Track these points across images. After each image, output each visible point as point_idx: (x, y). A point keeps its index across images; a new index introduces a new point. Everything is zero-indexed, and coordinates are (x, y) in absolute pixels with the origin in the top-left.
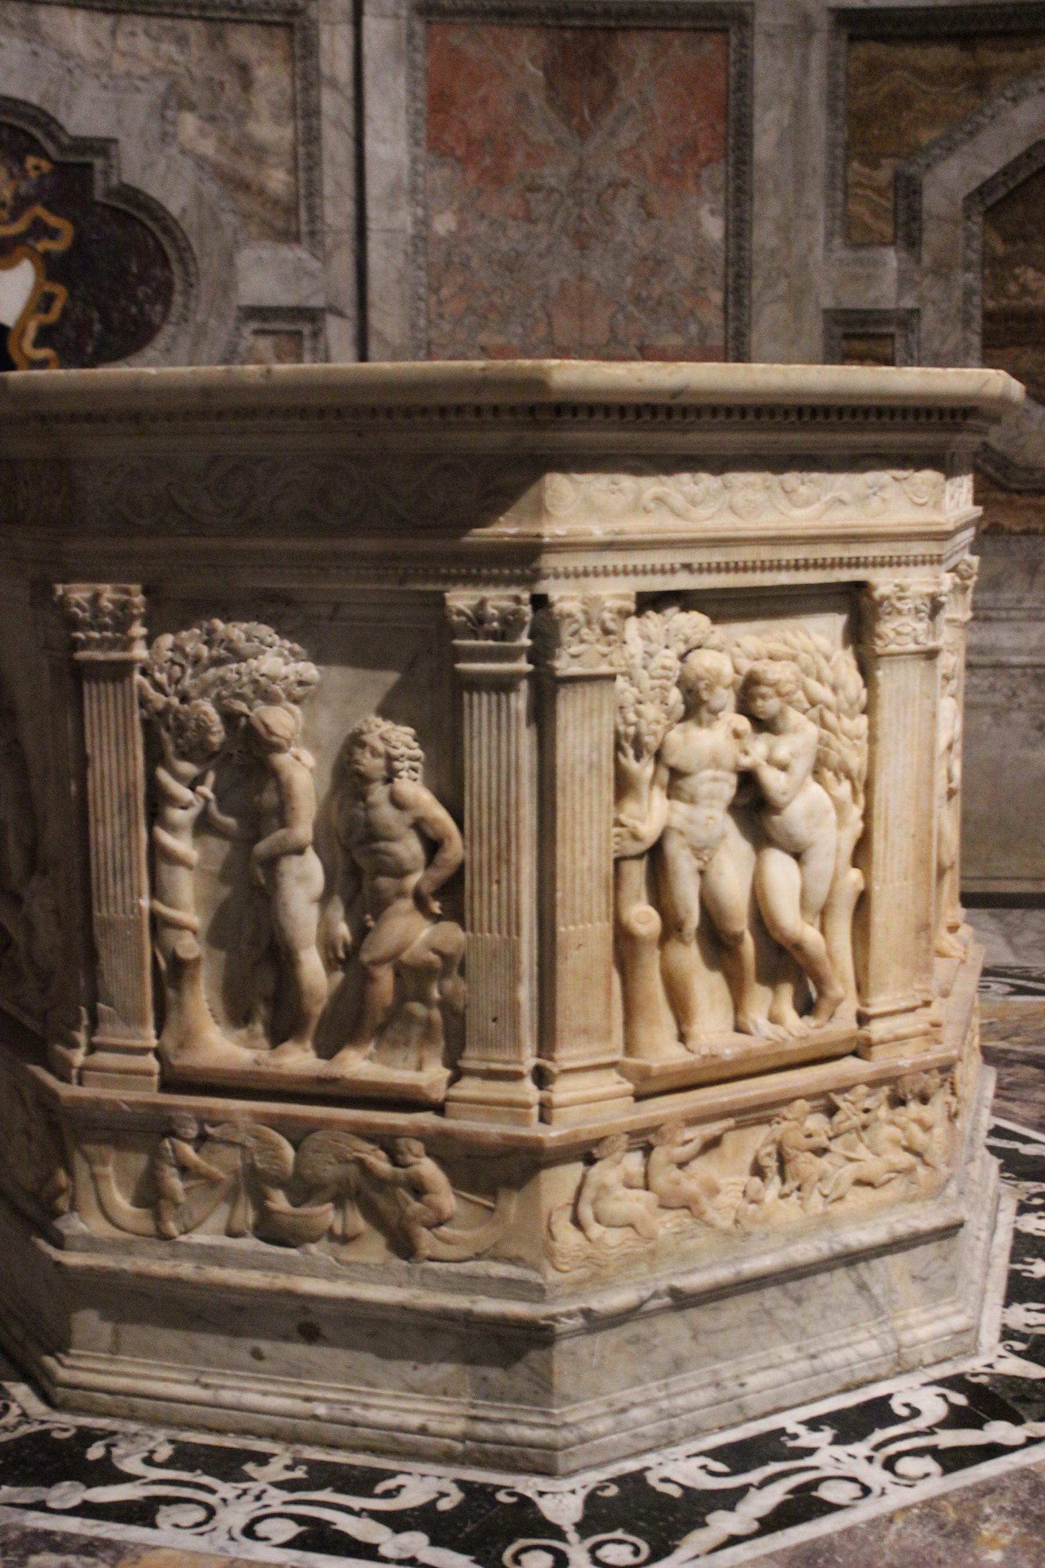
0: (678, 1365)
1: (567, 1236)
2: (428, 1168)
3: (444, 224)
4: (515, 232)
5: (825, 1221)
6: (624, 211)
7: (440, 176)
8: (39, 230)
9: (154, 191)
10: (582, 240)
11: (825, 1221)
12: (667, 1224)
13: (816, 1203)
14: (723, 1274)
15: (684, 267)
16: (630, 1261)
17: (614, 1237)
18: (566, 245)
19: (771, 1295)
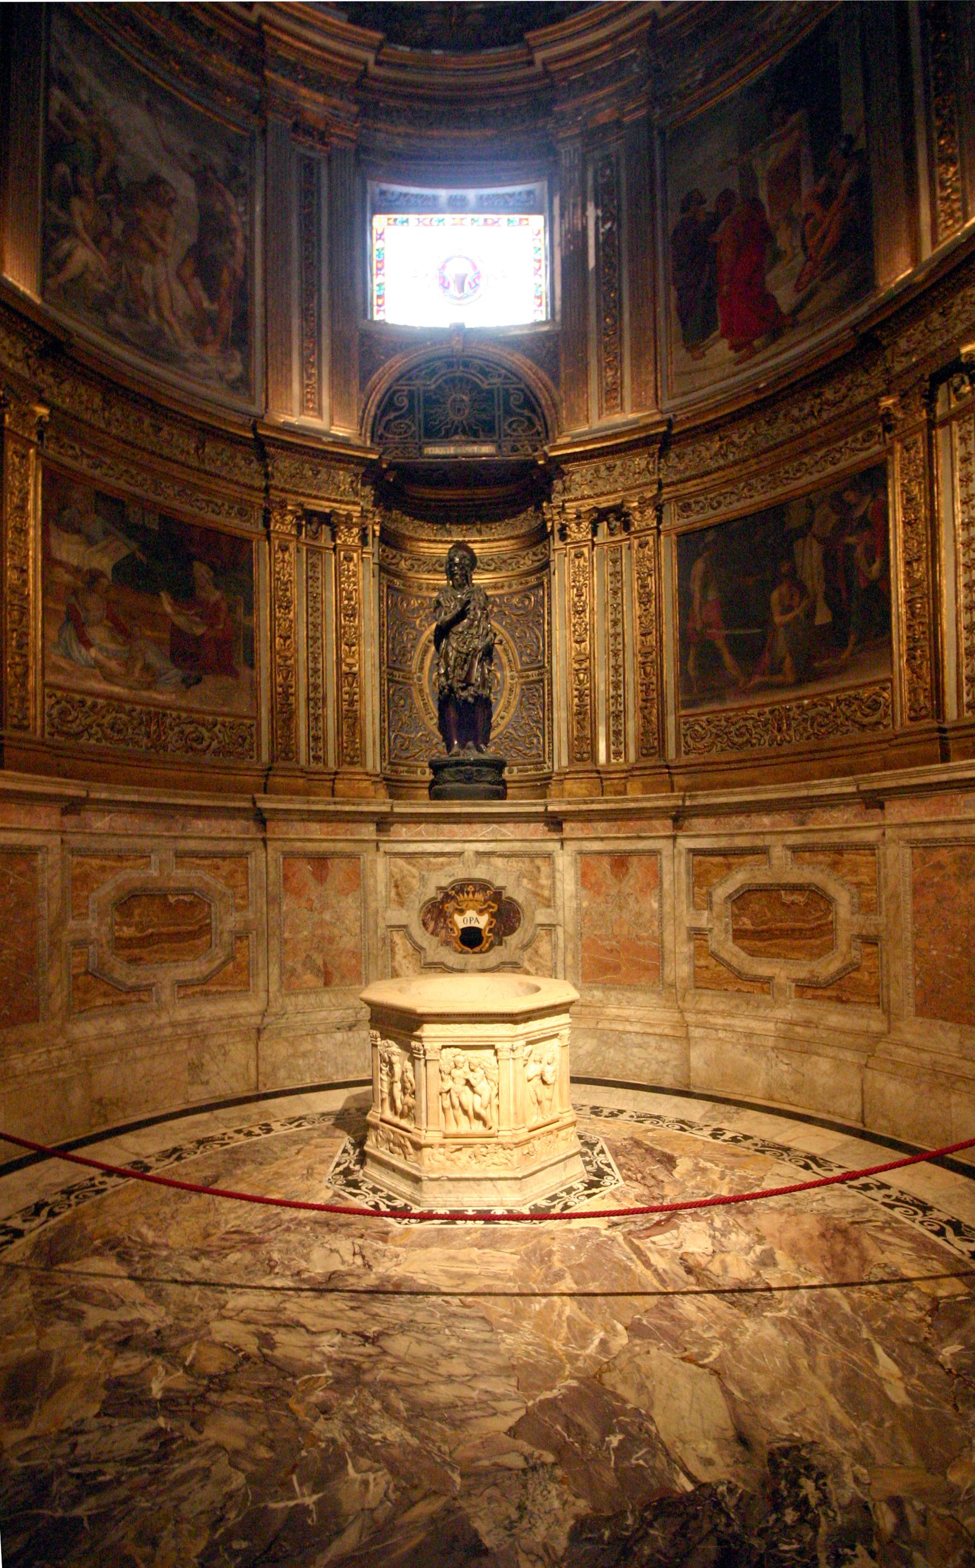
0: (450, 1192)
1: (427, 1162)
2: (408, 1144)
3: (585, 904)
4: (603, 906)
5: (485, 1170)
6: (631, 900)
7: (584, 892)
8: (490, 907)
9: (515, 897)
10: (621, 908)
11: (485, 1170)
12: (448, 1163)
13: (484, 1165)
14: (458, 1176)
15: (648, 916)
16: (439, 1169)
17: (436, 1164)
18: (617, 909)
19: (472, 1183)
